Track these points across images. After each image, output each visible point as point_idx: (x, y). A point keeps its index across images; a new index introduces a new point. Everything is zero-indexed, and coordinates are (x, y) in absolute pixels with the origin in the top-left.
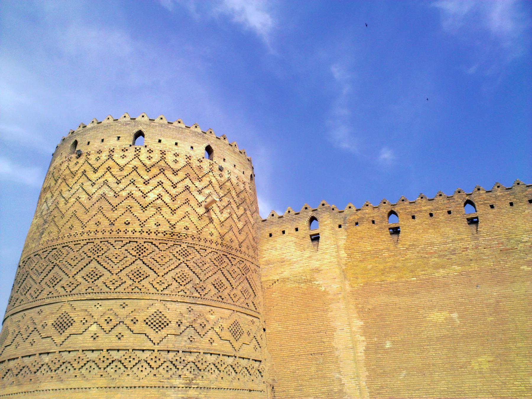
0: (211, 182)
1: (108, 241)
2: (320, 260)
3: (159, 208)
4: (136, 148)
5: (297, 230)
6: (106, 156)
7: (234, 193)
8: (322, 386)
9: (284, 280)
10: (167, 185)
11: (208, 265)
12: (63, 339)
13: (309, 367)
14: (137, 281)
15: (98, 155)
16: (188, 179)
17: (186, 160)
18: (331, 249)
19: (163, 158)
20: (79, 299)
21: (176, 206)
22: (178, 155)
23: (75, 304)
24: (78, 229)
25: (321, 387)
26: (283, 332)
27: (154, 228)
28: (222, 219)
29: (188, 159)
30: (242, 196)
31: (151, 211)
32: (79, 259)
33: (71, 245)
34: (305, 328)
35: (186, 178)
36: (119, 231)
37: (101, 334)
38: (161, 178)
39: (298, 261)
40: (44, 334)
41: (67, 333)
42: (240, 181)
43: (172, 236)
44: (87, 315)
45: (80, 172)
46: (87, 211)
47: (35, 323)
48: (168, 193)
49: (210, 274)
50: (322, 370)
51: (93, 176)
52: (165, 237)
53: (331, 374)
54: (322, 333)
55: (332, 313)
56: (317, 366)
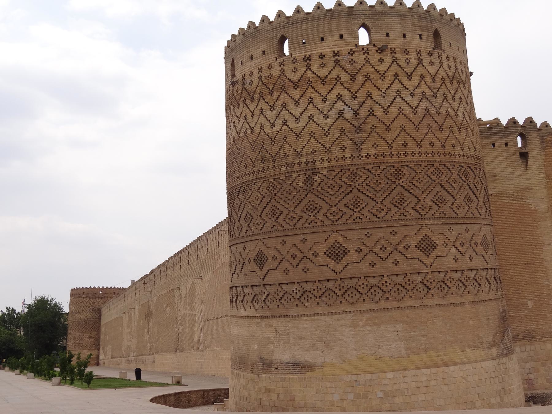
1: (444, 165)
2: (530, 180)
5: (506, 144)
6: (415, 59)
8: (535, 290)
9: (498, 195)
12: (432, 260)
13: (523, 274)
15: (407, 56)
18: (539, 169)
20: (436, 223)
23: (433, 228)
24: (412, 147)
25: (534, 291)
26: (500, 243)
32: (424, 181)
33: (412, 165)
34: (518, 241)
37: (459, 256)
39: (509, 178)
40: (410, 255)
41: (433, 254)
44: (446, 239)
45: (391, 73)
46: (417, 128)
47: (391, 244)
50: (534, 278)
53: (541, 281)
54: (533, 247)
55: (540, 230)
56: (530, 274)
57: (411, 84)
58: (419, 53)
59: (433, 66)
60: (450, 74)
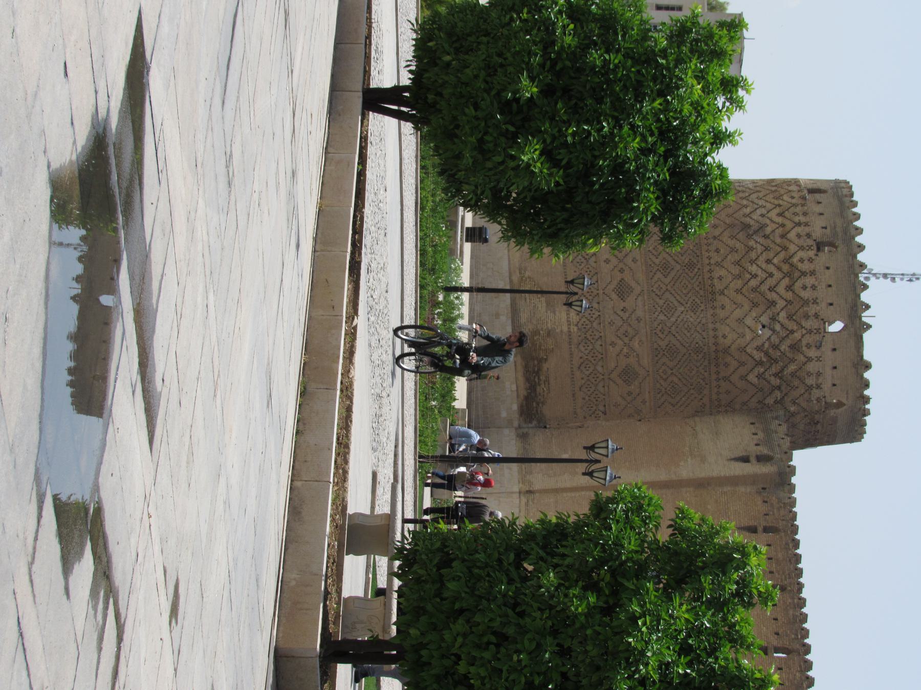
0: (792, 332)
3: (739, 276)
4: (812, 246)
6: (799, 220)
7: (792, 367)
10: (771, 282)
14: (659, 268)
15: (801, 214)
17: (810, 299)
19: (804, 274)
22: (814, 289)
27: (716, 274)
28: (749, 350)
30: (796, 383)
31: (736, 270)
36: (708, 245)
38: (778, 275)
42: (817, 379)
51: (773, 215)
57: (773, 215)
58: (806, 224)
59: (797, 238)
60: (795, 260)
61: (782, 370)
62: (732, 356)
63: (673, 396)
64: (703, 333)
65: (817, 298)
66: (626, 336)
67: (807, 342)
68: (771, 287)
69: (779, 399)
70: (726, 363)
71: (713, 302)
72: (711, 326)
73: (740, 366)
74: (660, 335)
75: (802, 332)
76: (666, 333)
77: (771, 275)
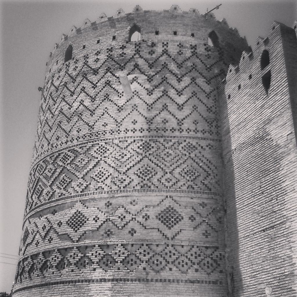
0: (136, 66)
7: (173, 66)
11: (129, 155)
16: (109, 74)
19: (86, 63)
21: (94, 106)
29: (109, 52)
35: (107, 73)
43: (91, 137)
48: (89, 96)
49: (131, 165)
52: (84, 140)
60: (74, 74)
61: (175, 75)
62: (155, 116)
63: (196, 174)
64: (129, 142)
65: (108, 49)
66: (124, 217)
67: (147, 54)
68: (93, 87)
69: (205, 80)
70: (163, 121)
71: (99, 134)
72: (122, 134)
73: (167, 110)
74: (126, 183)
75: (137, 58)
76: (124, 177)
77: (83, 89)
